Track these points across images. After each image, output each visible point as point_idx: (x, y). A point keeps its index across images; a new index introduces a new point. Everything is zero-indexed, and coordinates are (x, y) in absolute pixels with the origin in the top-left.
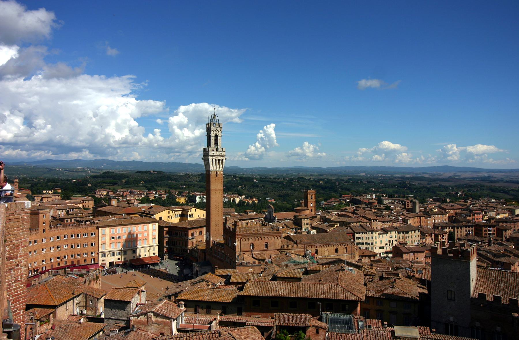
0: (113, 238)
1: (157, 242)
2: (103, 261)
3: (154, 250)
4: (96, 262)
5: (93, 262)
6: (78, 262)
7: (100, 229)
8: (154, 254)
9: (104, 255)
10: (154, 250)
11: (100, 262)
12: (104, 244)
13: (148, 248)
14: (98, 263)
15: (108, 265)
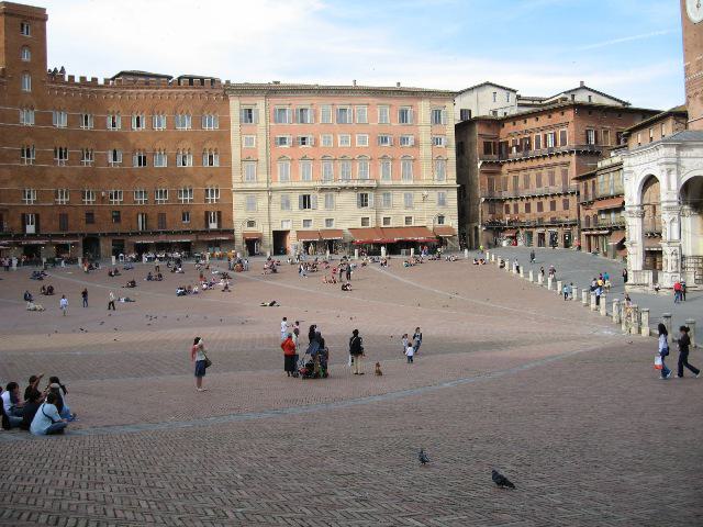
0: (283, 141)
1: (453, 174)
2: (251, 224)
3: (442, 203)
4: (224, 227)
5: (213, 226)
6: (162, 216)
7: (235, 106)
8: (441, 219)
9: (251, 205)
10: (442, 203)
11: (240, 230)
12: (248, 160)
13: (418, 195)
14: (232, 232)
15: (269, 240)
